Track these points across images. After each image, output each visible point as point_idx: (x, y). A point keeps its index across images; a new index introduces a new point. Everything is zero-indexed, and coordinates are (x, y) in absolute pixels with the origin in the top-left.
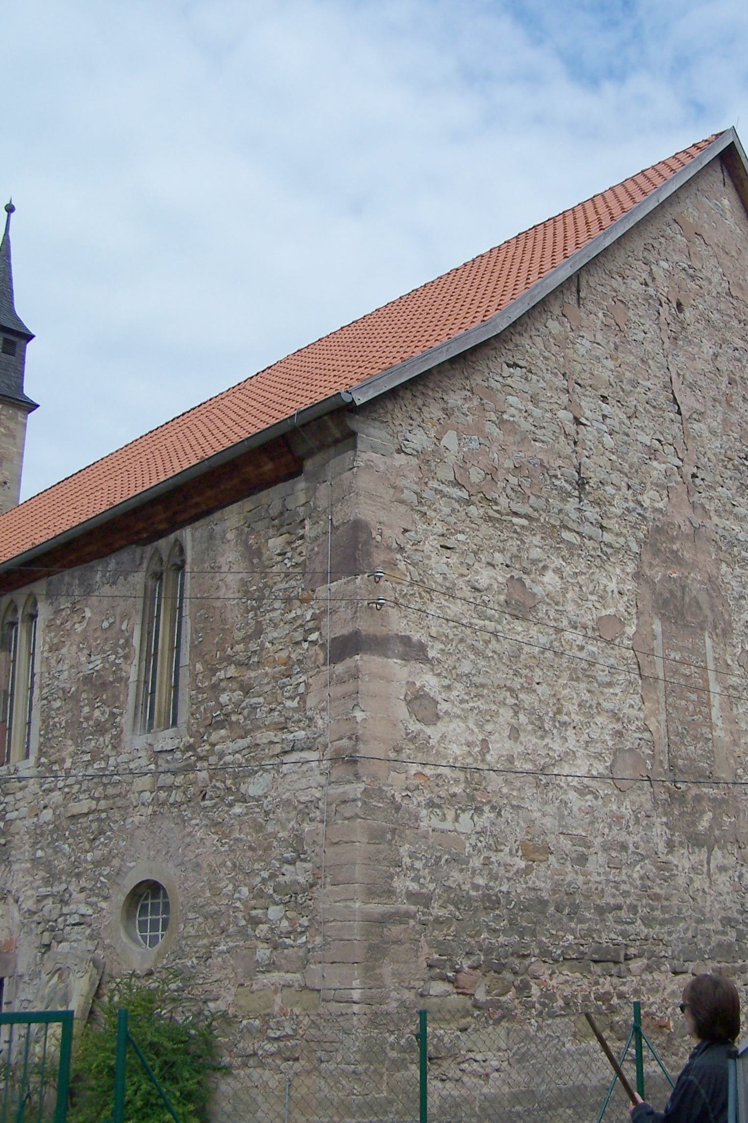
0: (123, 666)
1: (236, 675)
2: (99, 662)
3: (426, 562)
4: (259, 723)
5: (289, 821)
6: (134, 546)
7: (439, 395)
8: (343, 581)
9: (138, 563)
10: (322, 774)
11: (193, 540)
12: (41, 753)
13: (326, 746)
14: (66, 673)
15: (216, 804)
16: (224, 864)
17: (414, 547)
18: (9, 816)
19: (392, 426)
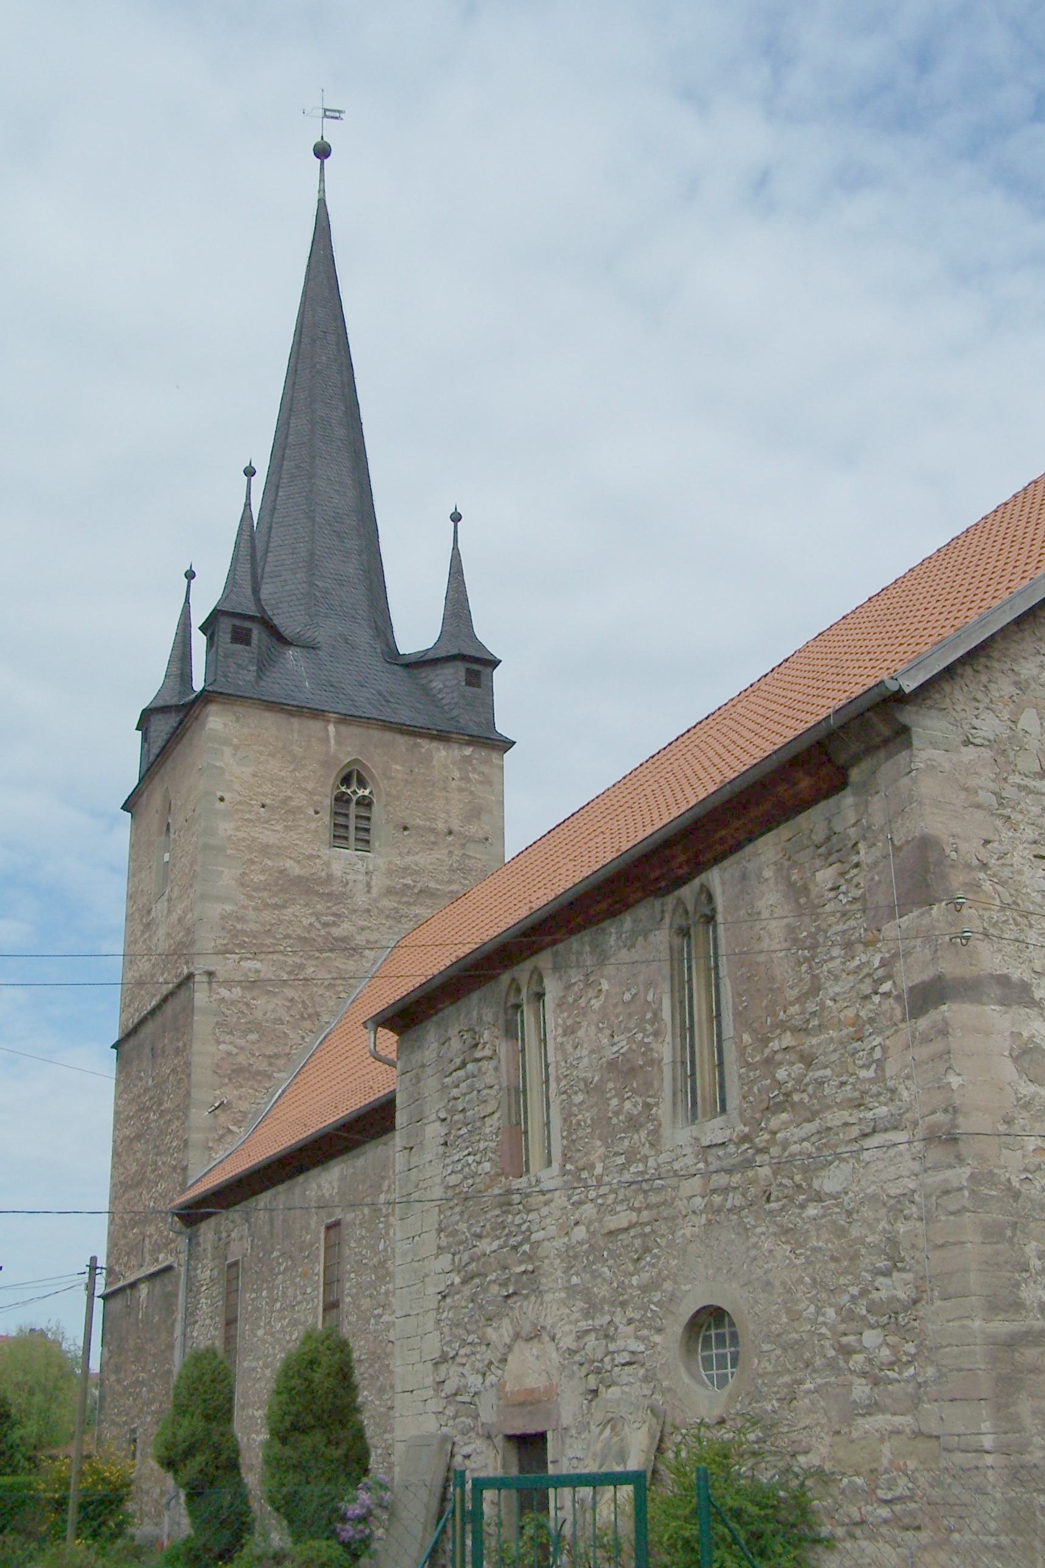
0: (654, 1046)
1: (793, 1043)
2: (625, 1043)
3: (1017, 878)
4: (829, 1101)
5: (878, 1220)
6: (651, 898)
7: (1008, 666)
8: (916, 913)
9: (658, 919)
10: (914, 1159)
11: (723, 884)
12: (566, 1158)
13: (915, 1124)
14: (586, 1061)
16: (801, 1280)
17: (1000, 862)
18: (534, 1237)
19: (954, 713)
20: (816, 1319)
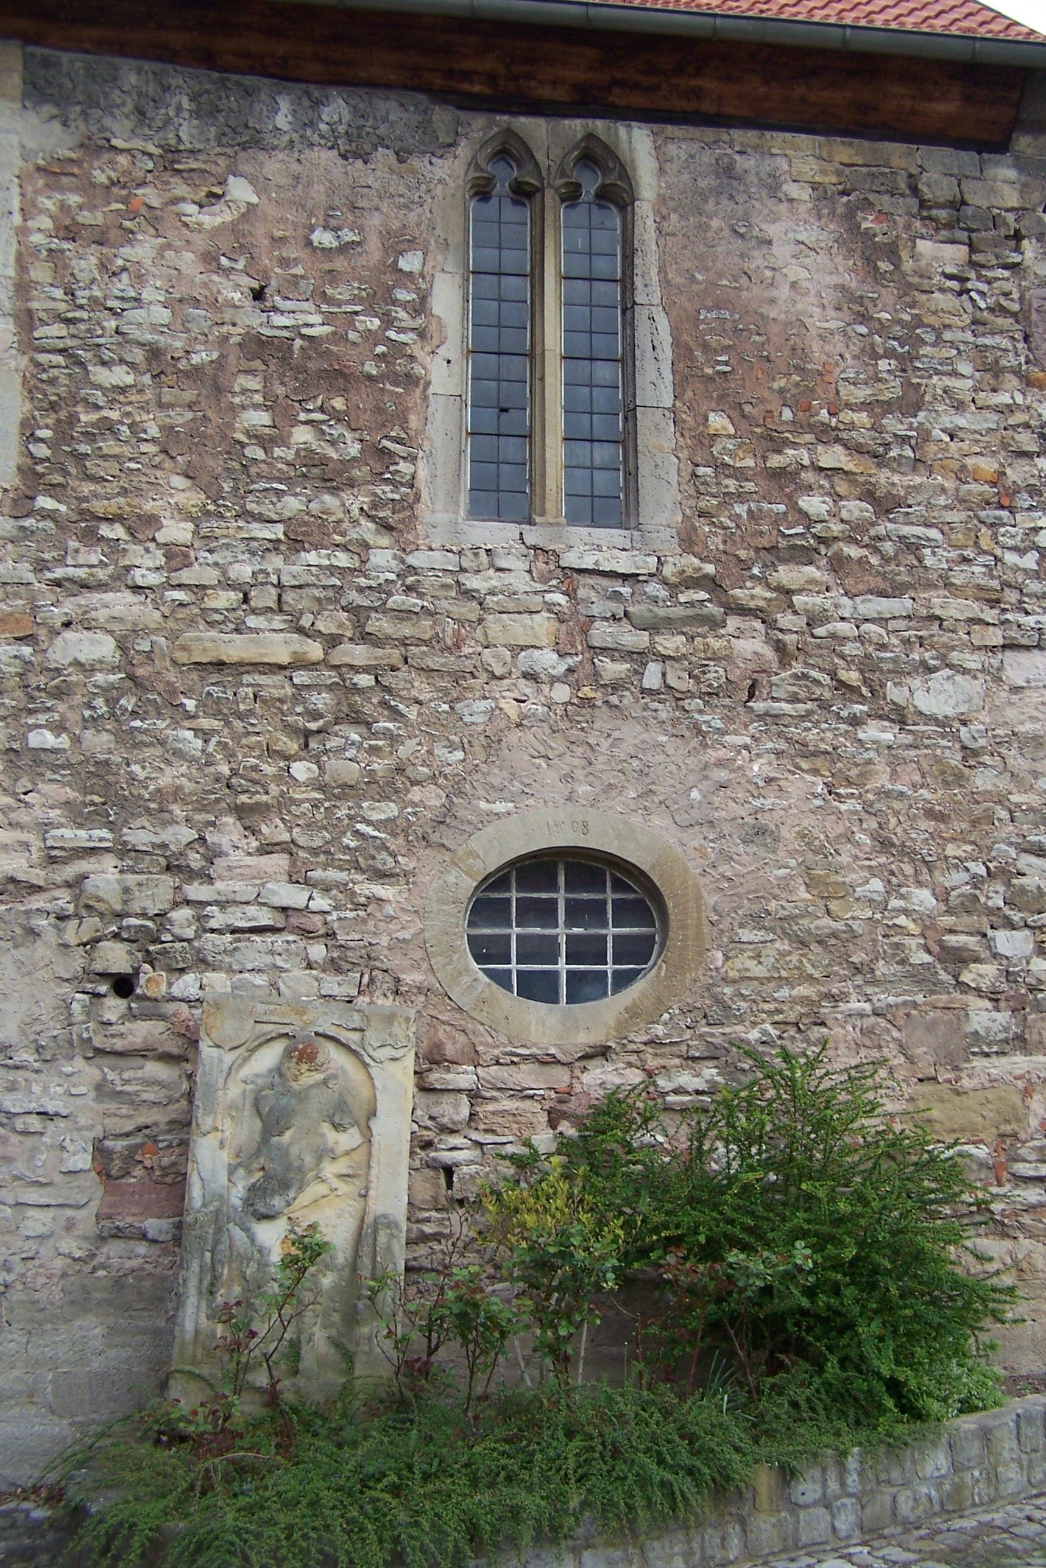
0: (417, 351)
1: (850, 467)
6: (423, 97)
15: (809, 713)
20: (887, 903)
